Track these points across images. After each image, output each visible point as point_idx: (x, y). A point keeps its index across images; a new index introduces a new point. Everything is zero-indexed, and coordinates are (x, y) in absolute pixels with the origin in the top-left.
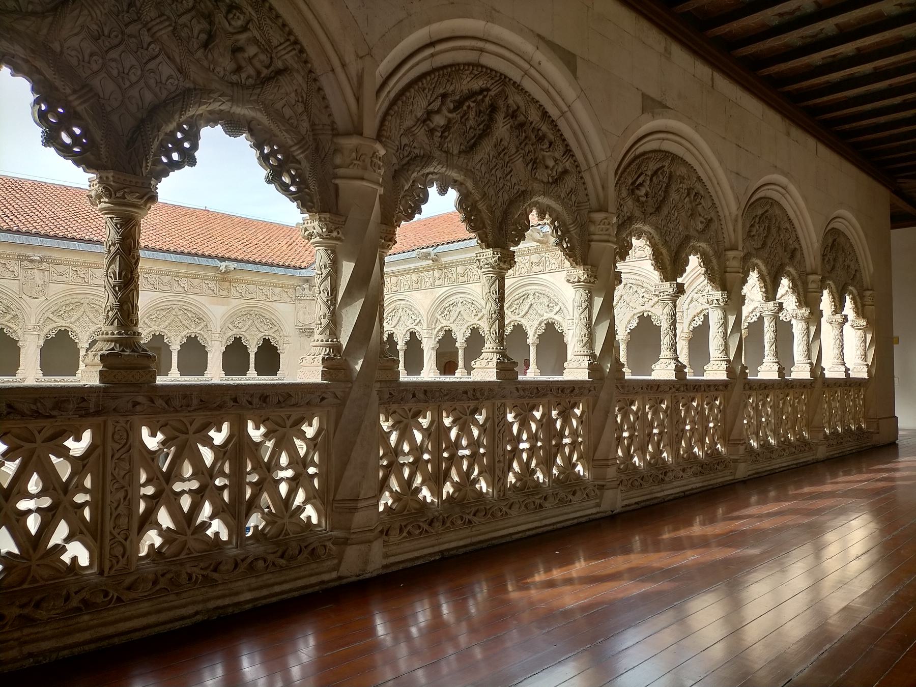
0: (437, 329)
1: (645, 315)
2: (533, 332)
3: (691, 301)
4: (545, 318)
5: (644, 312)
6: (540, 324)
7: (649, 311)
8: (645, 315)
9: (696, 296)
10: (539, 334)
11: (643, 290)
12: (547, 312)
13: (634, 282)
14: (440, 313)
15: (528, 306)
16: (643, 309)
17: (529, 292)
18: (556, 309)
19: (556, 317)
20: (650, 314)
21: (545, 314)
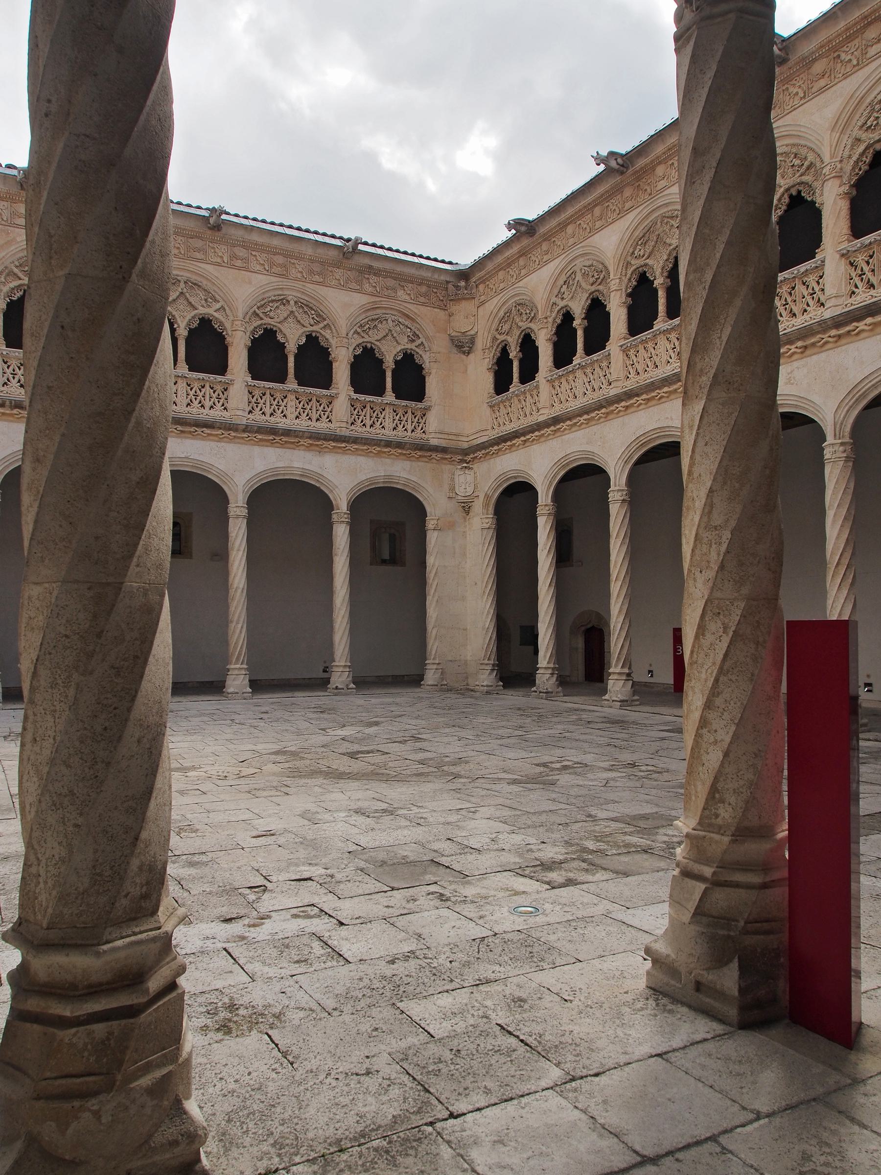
0: (12, 285)
1: (314, 335)
2: (185, 323)
3: (354, 333)
4: (201, 312)
5: (314, 331)
6: (193, 317)
7: (317, 332)
8: (314, 335)
9: (359, 330)
10: (191, 327)
11: (313, 312)
12: (203, 306)
13: (305, 302)
14: (17, 263)
15: (178, 293)
16: (311, 329)
17: (179, 278)
18: (218, 306)
19: (215, 314)
20: (318, 335)
21: (201, 308)
